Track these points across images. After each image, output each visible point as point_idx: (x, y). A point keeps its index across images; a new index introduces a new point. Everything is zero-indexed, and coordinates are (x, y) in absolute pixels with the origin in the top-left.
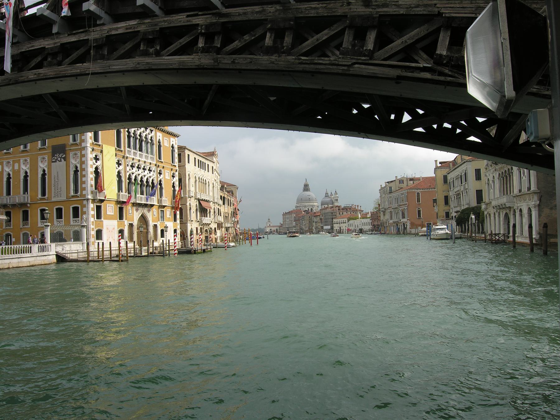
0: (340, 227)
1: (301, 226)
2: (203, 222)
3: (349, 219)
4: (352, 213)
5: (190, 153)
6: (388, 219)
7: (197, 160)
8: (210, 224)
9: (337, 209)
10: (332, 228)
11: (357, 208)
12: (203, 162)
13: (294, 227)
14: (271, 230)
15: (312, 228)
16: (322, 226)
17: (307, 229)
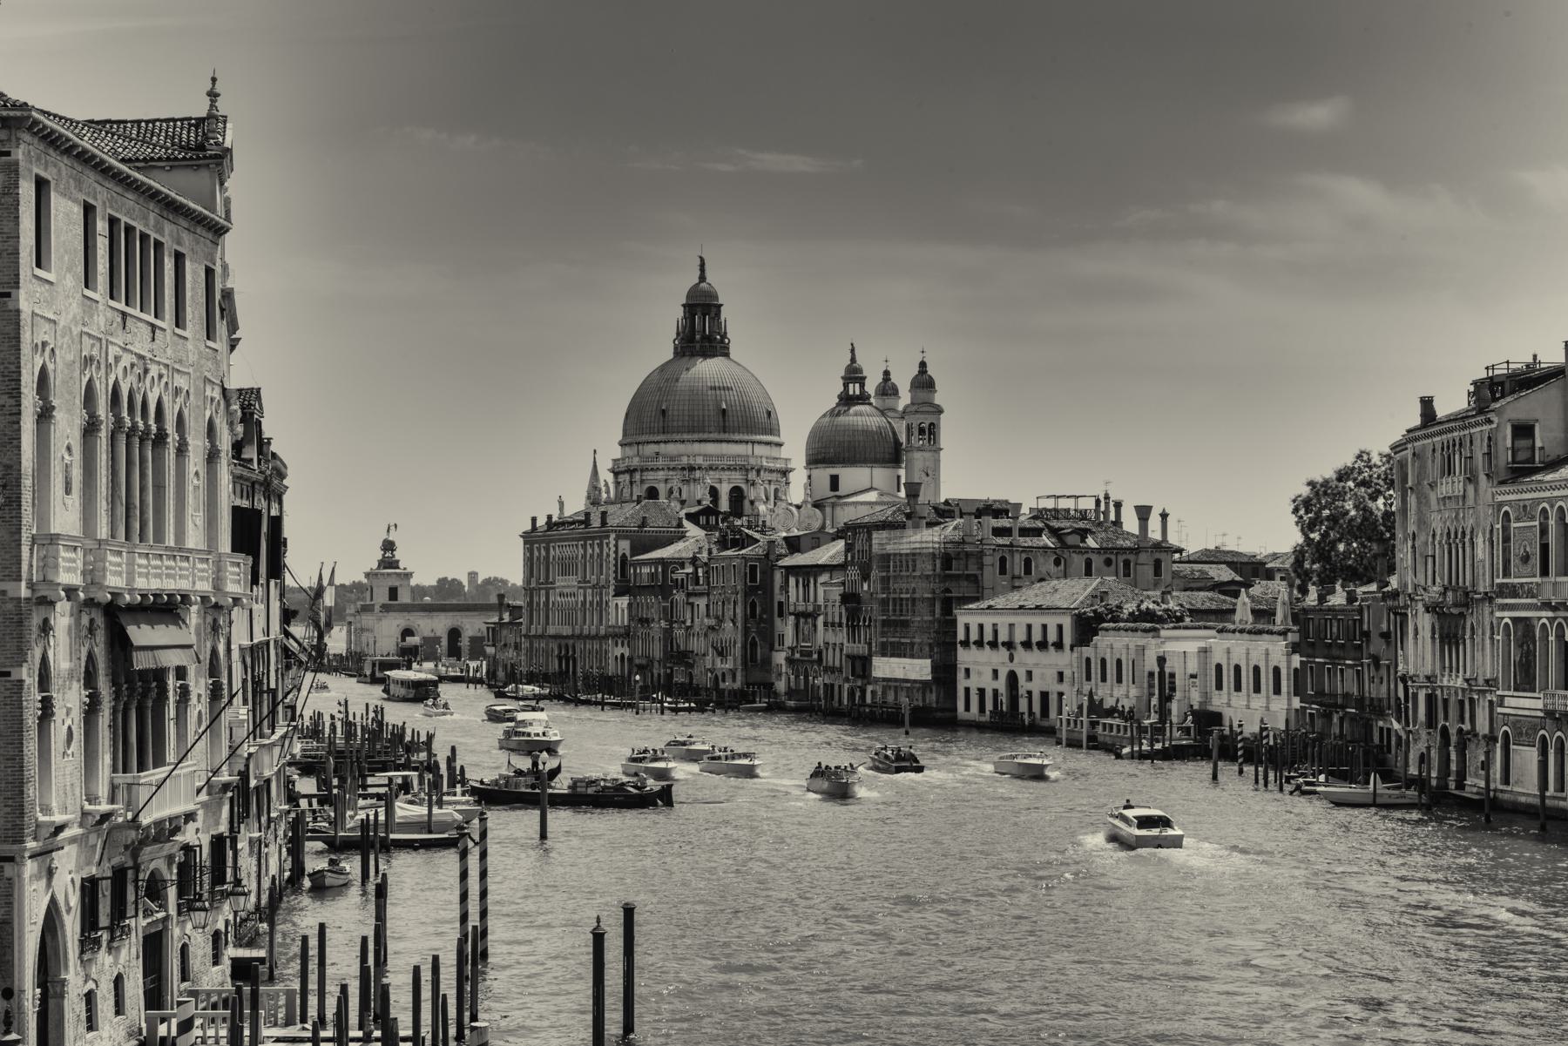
0: (1012, 678)
1: (679, 632)
2: (145, 820)
3: (1087, 627)
4: (1097, 561)
5: (57, 169)
6: (1487, 681)
7: (102, 226)
8: (190, 817)
9: (988, 533)
10: (945, 673)
11: (1131, 524)
12: (144, 237)
13: (625, 635)
14: (408, 632)
15: (767, 662)
16: (860, 649)
17: (729, 665)
